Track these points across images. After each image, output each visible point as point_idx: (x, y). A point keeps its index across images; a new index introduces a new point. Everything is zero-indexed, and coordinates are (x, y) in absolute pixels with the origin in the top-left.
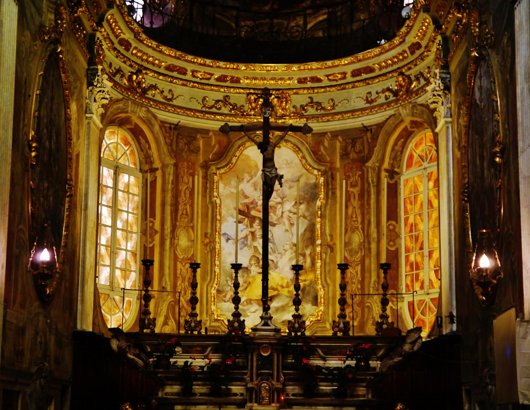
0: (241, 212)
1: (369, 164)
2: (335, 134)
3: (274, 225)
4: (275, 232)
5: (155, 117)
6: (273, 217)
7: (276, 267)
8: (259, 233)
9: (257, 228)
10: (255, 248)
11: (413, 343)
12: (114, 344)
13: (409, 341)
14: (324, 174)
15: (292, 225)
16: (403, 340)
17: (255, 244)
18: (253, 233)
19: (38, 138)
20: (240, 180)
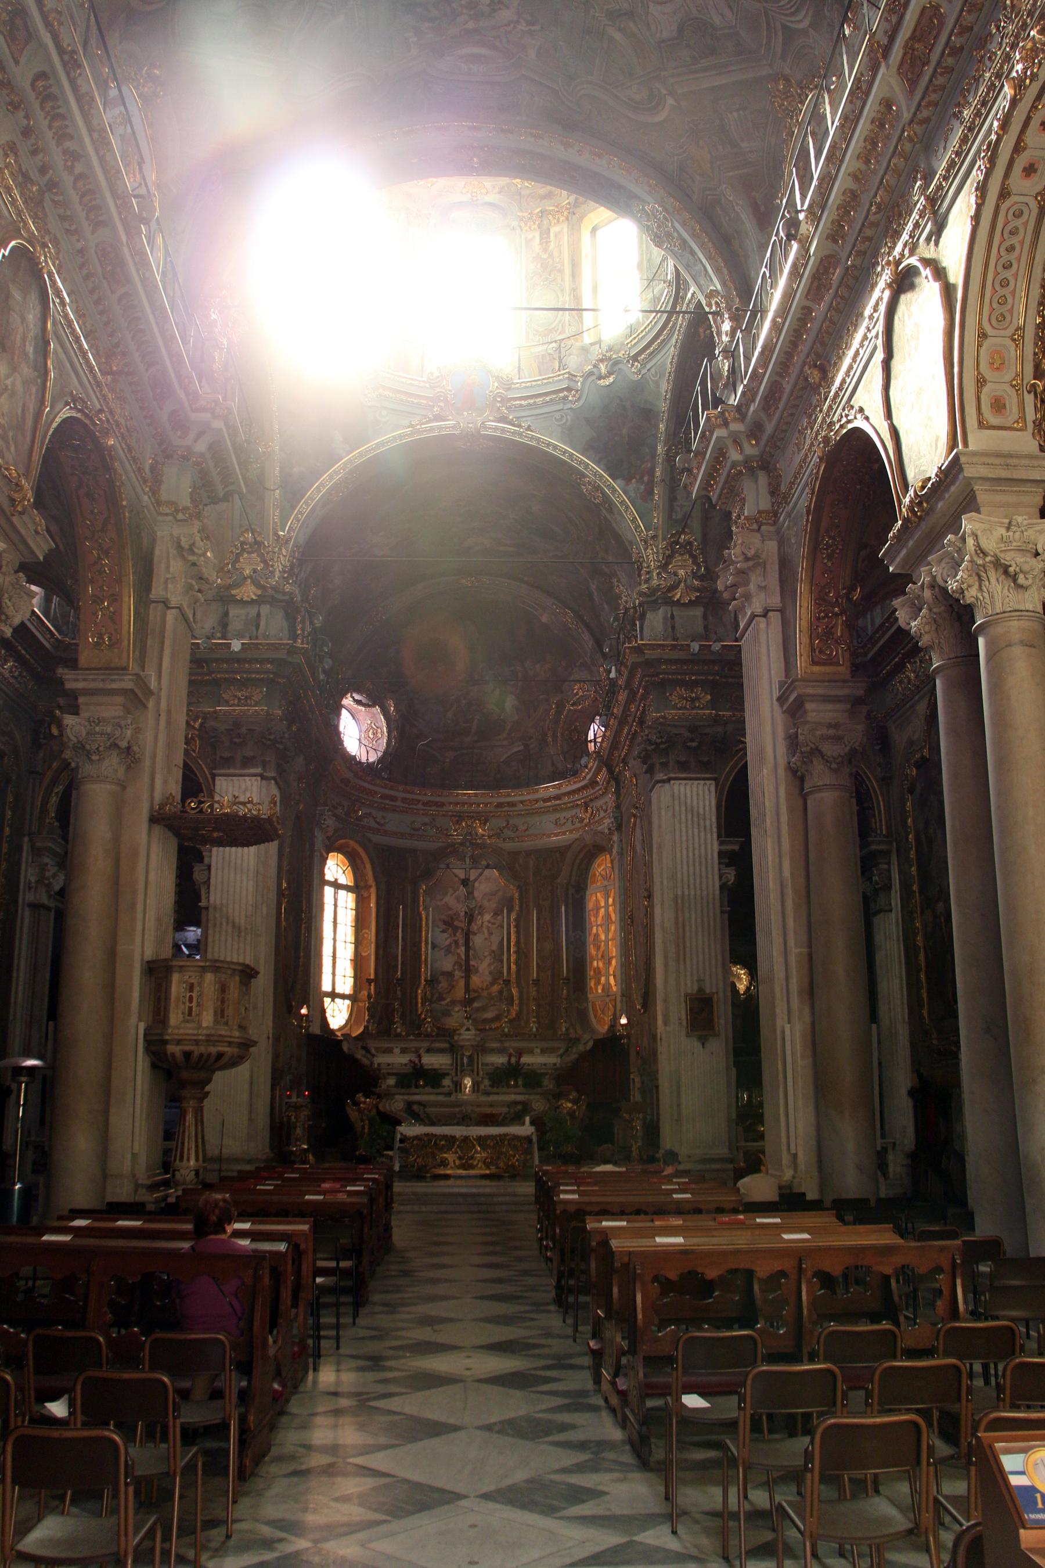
0: (445, 923)
1: (559, 880)
2: (529, 853)
3: (475, 934)
4: (477, 940)
5: (370, 840)
6: (474, 927)
7: (477, 971)
8: (461, 941)
9: (460, 936)
10: (458, 954)
11: (585, 1044)
12: (345, 1047)
13: (583, 1042)
14: (519, 887)
15: (491, 934)
16: (578, 1040)
17: (459, 951)
18: (456, 942)
19: (288, 888)
20: (445, 894)
